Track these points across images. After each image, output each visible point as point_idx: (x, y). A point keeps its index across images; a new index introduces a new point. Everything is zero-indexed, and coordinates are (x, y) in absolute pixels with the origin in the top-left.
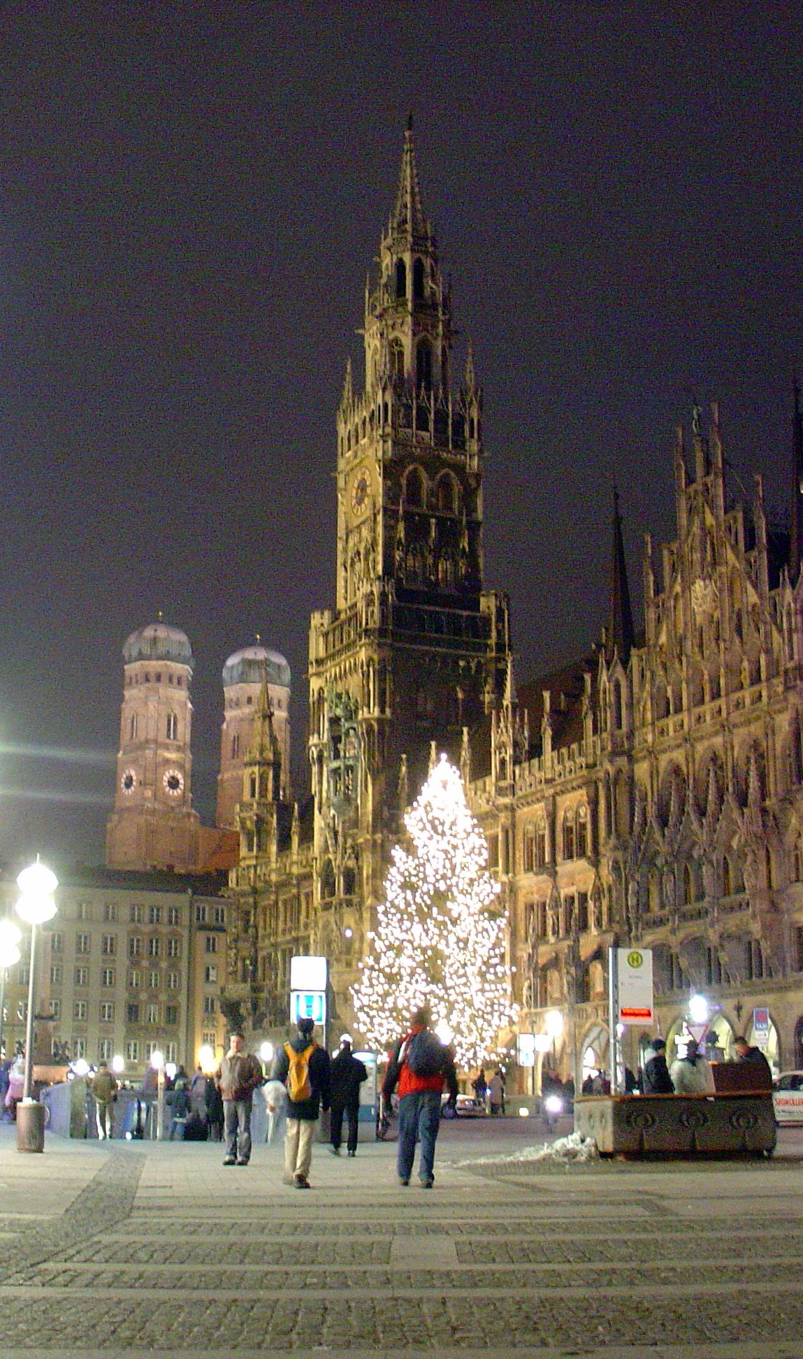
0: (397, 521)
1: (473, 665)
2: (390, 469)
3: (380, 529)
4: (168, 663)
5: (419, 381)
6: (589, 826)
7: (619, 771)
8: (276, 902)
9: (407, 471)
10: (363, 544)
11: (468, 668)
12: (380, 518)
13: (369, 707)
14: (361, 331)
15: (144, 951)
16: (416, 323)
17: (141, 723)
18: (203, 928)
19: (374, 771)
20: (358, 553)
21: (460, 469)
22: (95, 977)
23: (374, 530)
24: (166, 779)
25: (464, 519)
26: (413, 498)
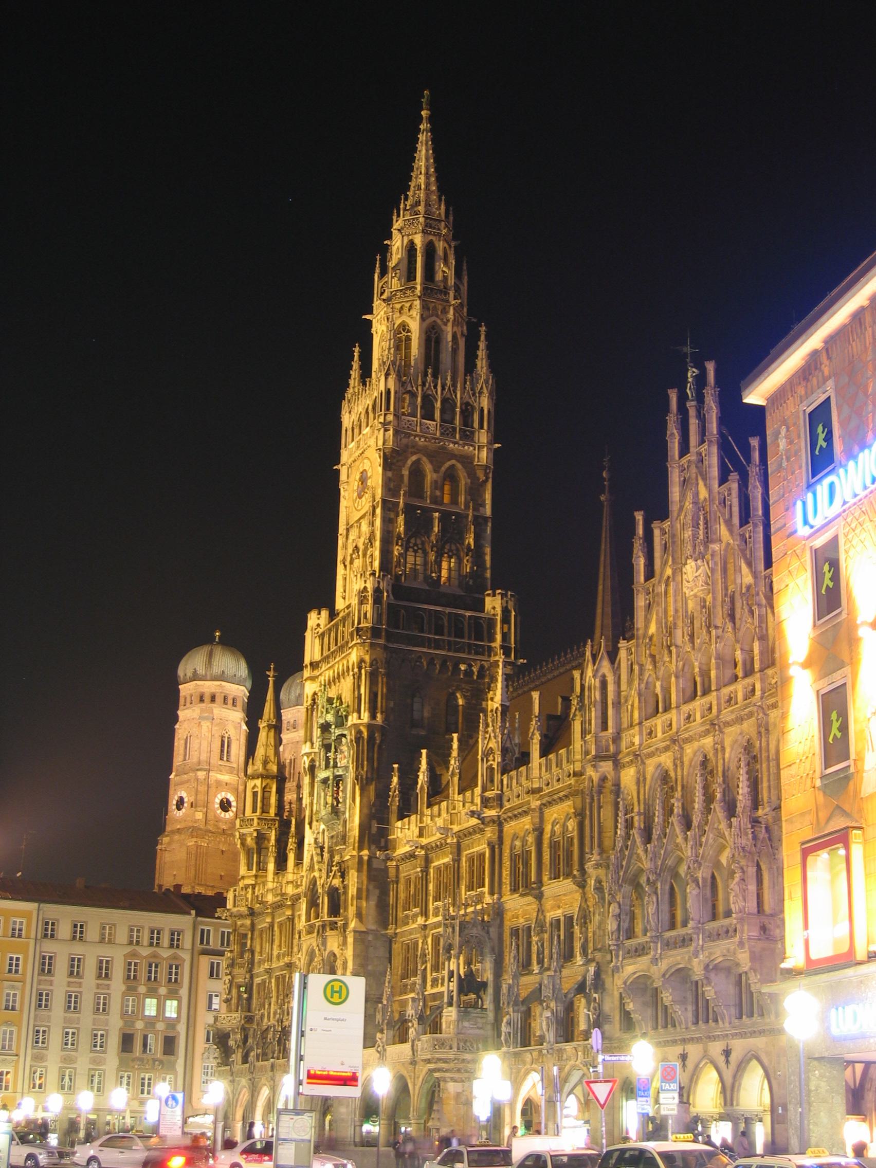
0: (397, 516)
1: (475, 670)
2: (390, 461)
3: (378, 522)
4: (223, 683)
5: (426, 367)
6: (576, 841)
7: (604, 779)
8: (272, 925)
9: (409, 462)
10: (362, 540)
11: (468, 673)
12: (378, 511)
13: (359, 712)
14: (368, 317)
15: (143, 975)
16: (425, 307)
17: (194, 744)
18: (205, 952)
19: (363, 782)
20: (356, 548)
21: (467, 461)
22: (87, 1002)
23: (372, 524)
24: (218, 801)
25: (471, 513)
26: (416, 488)
